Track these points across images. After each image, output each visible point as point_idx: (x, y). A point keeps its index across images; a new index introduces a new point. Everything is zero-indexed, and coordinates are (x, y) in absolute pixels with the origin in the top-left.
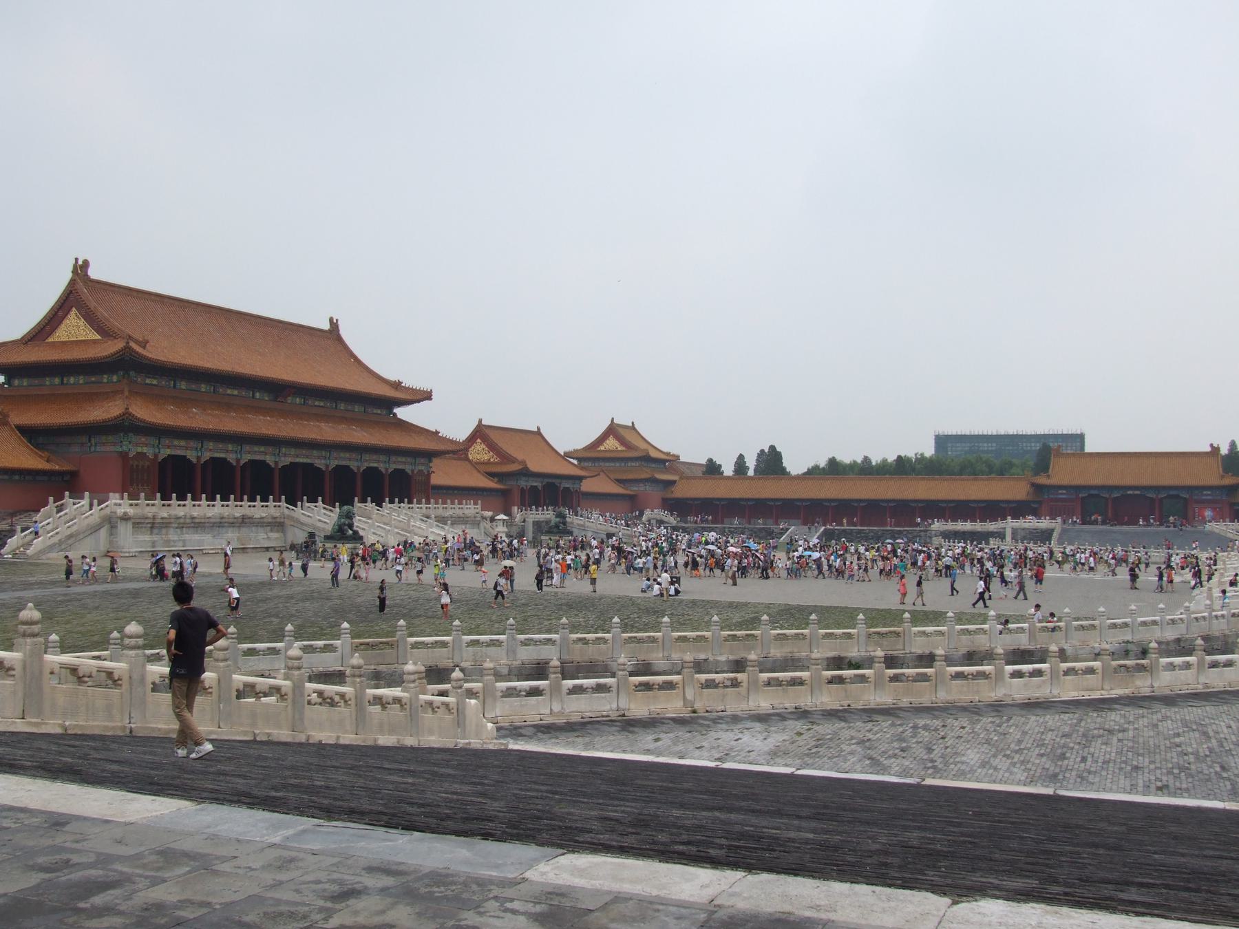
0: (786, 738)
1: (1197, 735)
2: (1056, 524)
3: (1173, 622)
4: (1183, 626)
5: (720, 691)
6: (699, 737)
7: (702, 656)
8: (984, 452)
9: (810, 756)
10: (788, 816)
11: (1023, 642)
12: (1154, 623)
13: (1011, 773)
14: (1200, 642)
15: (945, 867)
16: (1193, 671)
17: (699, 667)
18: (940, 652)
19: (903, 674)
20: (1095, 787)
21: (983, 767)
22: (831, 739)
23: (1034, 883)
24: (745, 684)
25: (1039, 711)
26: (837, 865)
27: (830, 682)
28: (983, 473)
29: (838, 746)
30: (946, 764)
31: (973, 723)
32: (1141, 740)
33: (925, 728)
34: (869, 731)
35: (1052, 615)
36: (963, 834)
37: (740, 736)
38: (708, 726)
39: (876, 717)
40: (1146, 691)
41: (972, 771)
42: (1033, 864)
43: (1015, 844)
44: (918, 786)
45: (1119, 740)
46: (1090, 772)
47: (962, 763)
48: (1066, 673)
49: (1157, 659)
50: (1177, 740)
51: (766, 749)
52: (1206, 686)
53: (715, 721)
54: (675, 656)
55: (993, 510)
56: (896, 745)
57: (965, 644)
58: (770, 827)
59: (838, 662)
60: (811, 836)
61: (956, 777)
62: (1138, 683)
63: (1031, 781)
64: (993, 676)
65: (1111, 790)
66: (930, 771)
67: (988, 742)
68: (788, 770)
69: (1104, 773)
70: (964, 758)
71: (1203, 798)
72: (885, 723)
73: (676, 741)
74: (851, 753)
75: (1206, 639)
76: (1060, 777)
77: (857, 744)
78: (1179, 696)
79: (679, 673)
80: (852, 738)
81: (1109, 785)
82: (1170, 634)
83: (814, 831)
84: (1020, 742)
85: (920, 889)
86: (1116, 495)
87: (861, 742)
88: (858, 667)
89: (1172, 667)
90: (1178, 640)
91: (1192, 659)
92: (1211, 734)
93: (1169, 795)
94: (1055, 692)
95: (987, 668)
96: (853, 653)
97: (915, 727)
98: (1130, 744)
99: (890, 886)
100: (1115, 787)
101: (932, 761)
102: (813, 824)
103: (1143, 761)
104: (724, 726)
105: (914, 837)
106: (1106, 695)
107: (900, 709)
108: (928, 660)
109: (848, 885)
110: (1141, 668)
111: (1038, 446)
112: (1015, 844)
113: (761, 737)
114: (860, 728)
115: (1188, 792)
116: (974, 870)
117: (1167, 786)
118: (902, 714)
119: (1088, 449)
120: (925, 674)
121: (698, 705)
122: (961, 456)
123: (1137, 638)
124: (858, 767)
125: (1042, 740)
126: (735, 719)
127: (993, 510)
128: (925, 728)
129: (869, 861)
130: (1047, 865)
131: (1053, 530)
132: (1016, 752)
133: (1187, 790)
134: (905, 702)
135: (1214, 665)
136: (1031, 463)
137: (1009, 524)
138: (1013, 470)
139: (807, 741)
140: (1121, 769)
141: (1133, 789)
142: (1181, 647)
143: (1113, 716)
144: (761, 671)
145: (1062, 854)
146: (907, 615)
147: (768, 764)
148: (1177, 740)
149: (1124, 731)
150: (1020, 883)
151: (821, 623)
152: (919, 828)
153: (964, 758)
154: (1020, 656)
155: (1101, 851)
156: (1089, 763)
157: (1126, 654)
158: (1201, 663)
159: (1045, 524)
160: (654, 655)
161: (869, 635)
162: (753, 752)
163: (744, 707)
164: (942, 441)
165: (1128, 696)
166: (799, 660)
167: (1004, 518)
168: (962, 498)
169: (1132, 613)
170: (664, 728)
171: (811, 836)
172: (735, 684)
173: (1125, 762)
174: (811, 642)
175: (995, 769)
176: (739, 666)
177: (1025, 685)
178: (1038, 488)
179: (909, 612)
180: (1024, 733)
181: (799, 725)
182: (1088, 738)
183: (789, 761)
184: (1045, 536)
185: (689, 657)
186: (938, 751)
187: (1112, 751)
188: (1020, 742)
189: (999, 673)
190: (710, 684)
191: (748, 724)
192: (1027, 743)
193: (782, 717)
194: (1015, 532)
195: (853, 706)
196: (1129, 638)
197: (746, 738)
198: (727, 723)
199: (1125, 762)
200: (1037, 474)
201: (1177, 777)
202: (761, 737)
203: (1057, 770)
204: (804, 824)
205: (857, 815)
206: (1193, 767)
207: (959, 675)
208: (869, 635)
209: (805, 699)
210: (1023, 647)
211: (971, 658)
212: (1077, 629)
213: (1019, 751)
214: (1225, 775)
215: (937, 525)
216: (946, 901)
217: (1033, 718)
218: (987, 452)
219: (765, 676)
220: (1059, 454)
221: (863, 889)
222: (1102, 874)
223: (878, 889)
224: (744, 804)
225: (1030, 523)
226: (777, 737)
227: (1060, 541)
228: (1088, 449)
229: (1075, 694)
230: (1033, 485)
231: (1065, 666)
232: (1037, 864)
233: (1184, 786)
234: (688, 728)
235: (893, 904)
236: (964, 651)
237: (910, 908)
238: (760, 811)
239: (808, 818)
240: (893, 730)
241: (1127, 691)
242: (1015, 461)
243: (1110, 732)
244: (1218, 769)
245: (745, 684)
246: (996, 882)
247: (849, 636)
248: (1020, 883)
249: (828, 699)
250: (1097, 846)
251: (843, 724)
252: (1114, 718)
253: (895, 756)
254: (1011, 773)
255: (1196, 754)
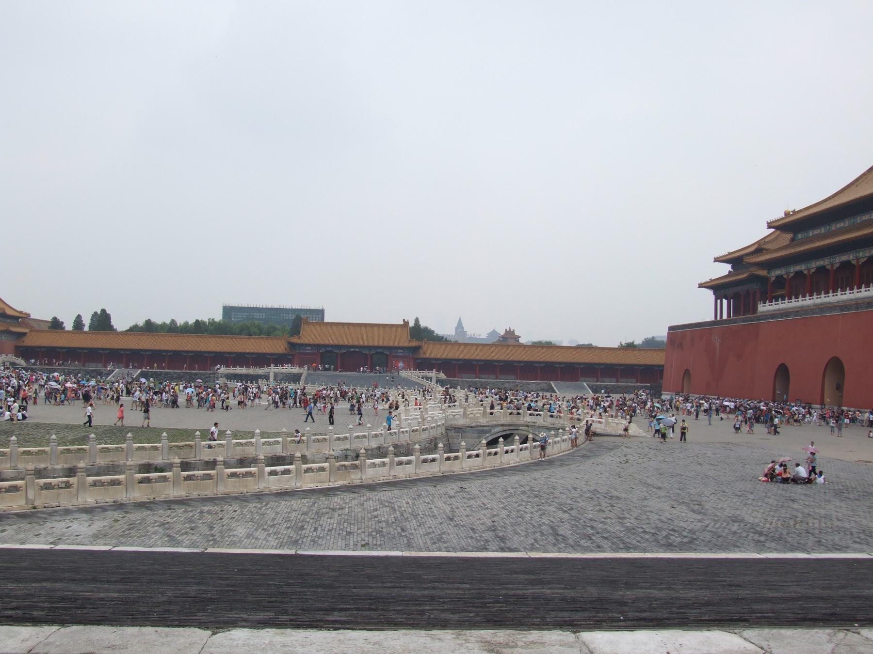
0: (106, 524)
1: (388, 509)
2: (304, 370)
3: (376, 435)
4: (382, 439)
5: (55, 491)
6: (38, 527)
7: (43, 466)
8: (256, 319)
9: (124, 536)
10: (101, 582)
11: (278, 451)
12: (364, 436)
13: (267, 541)
14: (391, 448)
15: (211, 609)
16: (387, 467)
17: (39, 473)
18: (220, 458)
19: (194, 475)
20: (322, 547)
21: (249, 538)
22: (140, 524)
23: (271, 615)
24: (75, 486)
25: (287, 498)
26: (132, 615)
27: (141, 482)
28: (255, 334)
29: (145, 528)
30: (223, 537)
31: (242, 507)
32: (353, 514)
33: (209, 512)
34: (168, 516)
35: (297, 431)
36: (228, 586)
37: (71, 524)
38: (45, 518)
39: (173, 506)
40: (357, 482)
41: (240, 541)
42: (272, 602)
43: (262, 590)
44: (202, 554)
45: (339, 515)
46: (319, 538)
47: (234, 536)
48: (307, 471)
49: (365, 461)
50: (375, 513)
51: (91, 533)
52: (395, 477)
53: (51, 514)
54: (21, 466)
55: (262, 360)
56: (187, 525)
57: (238, 453)
58: (84, 590)
59: (147, 468)
60: (116, 595)
61: (229, 546)
62: (353, 477)
63: (281, 546)
64: (257, 474)
65: (333, 549)
66: (211, 543)
67: (252, 520)
68: (107, 548)
69: (328, 538)
70: (235, 533)
71: (390, 550)
72: (180, 510)
73: (18, 532)
74: (155, 533)
75: (396, 446)
76: (300, 542)
77: (159, 526)
78: (378, 484)
79: (23, 479)
80: (156, 522)
81: (331, 545)
82: (374, 444)
83: (119, 591)
84: (274, 519)
85: (190, 626)
86: (343, 351)
87: (162, 525)
88: (162, 470)
89: (374, 465)
90: (379, 448)
91: (386, 460)
92: (397, 508)
93: (369, 549)
94: (299, 484)
95: (253, 469)
96: (159, 460)
97: (201, 512)
98: (346, 517)
99: (168, 626)
100: (335, 547)
101: (213, 535)
102: (120, 586)
103: (354, 528)
104: (58, 518)
105: (192, 590)
106: (331, 485)
107: (191, 500)
108: (212, 464)
109: (138, 628)
110: (355, 467)
111: (293, 317)
112: (262, 590)
113: (87, 524)
114: (162, 515)
115: (381, 547)
116: (231, 610)
117: (368, 544)
118: (193, 503)
119: (326, 320)
120: (210, 475)
121: (37, 503)
122: (240, 322)
123: (353, 447)
124: (159, 542)
125: (288, 517)
126: (67, 512)
127: (262, 360)
128: (209, 512)
129: (156, 610)
130: (282, 602)
131: (301, 374)
132: (271, 526)
133: (380, 546)
134: (195, 494)
135: (400, 463)
136: (288, 328)
137: (273, 370)
138: (276, 333)
139: (122, 525)
140: (339, 534)
141: (347, 547)
142: (380, 452)
143: (336, 499)
144: (88, 476)
145: (293, 593)
146: (198, 433)
147: (91, 544)
148: (375, 513)
149: (342, 509)
150: (261, 616)
151: (134, 440)
152: (198, 584)
153: (235, 533)
154: (276, 460)
155: (320, 590)
156: (319, 531)
157: (346, 458)
158: (391, 463)
159: (296, 370)
160: (3, 466)
161: (171, 448)
162: (79, 536)
163: (74, 502)
164: (228, 311)
165: (346, 486)
166: (118, 466)
167: (269, 366)
168: (240, 350)
169: (350, 430)
170: (9, 521)
171: (116, 595)
172: (68, 485)
173: (342, 530)
174: (128, 454)
175: (257, 539)
176: (71, 472)
177: (279, 480)
178: (292, 345)
179: (200, 431)
180: (277, 513)
181: (117, 515)
182: (319, 515)
183: (108, 541)
184: (296, 378)
185: (31, 466)
186: (217, 528)
187: (334, 522)
188: (274, 519)
189: (261, 472)
190: (48, 487)
191: (77, 515)
192: (279, 519)
193: (104, 509)
194: (276, 375)
195: (157, 499)
196: (348, 447)
197: (75, 526)
198: (60, 515)
199: (342, 530)
200: (292, 336)
201: (374, 538)
202: (87, 524)
203: (298, 537)
204: (112, 587)
205: (153, 577)
206: (384, 530)
207: (233, 475)
208: (171, 448)
209: (122, 496)
210: (278, 454)
211: (243, 462)
212: (314, 441)
213: (273, 526)
214: (403, 534)
215: (223, 370)
216: (209, 632)
217: (283, 503)
218: (260, 319)
219: (91, 479)
220: (307, 323)
221: (149, 630)
222: (318, 605)
223: (159, 629)
224: (67, 575)
225: (288, 369)
226: (99, 524)
227: (306, 382)
228: (326, 320)
229: (312, 485)
230: (289, 343)
231: (305, 466)
232: (276, 602)
233: (379, 543)
234: (29, 521)
235: (169, 639)
236: (237, 457)
237: (182, 640)
238: (79, 580)
239: (116, 582)
240: (186, 515)
241: (345, 482)
242: (277, 326)
243: (334, 510)
244: (400, 531)
245: (75, 486)
246: (245, 616)
247: (156, 448)
248: (261, 616)
249: (138, 494)
250: (317, 586)
251: (149, 512)
252: (336, 500)
253: (186, 533)
254: (267, 541)
255: (387, 522)
